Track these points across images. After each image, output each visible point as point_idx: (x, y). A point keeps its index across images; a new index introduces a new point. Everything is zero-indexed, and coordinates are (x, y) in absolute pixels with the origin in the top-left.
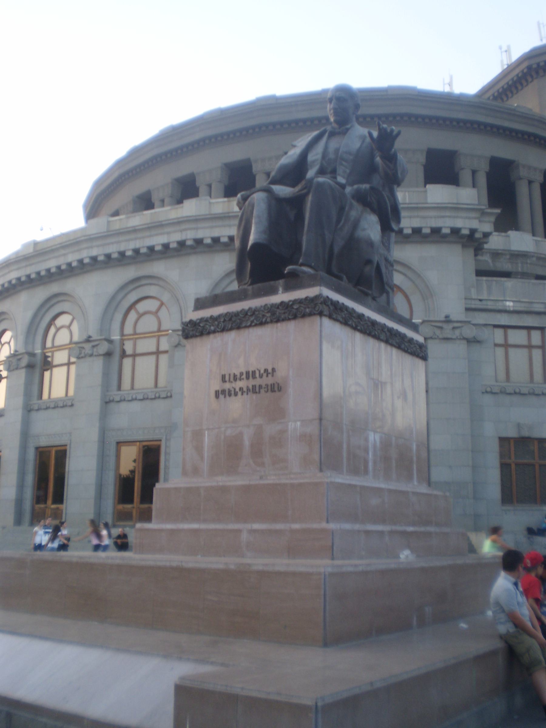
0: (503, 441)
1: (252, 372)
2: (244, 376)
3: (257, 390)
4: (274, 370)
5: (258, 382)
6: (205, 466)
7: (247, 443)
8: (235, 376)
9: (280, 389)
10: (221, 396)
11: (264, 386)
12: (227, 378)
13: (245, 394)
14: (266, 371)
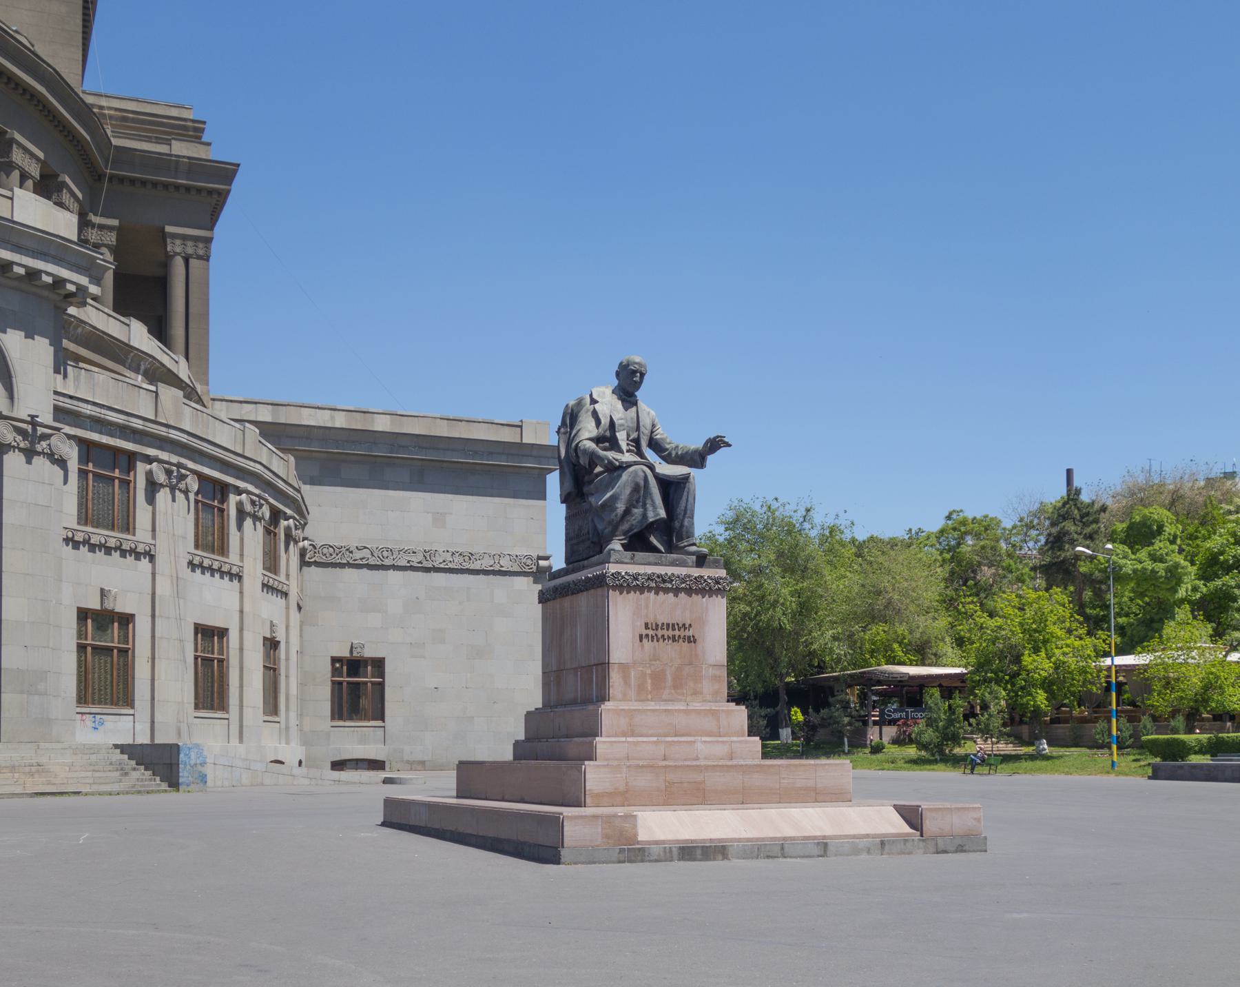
0: (83, 614)
5: (677, 633)
6: (632, 693)
7: (669, 677)
8: (657, 625)
10: (645, 640)
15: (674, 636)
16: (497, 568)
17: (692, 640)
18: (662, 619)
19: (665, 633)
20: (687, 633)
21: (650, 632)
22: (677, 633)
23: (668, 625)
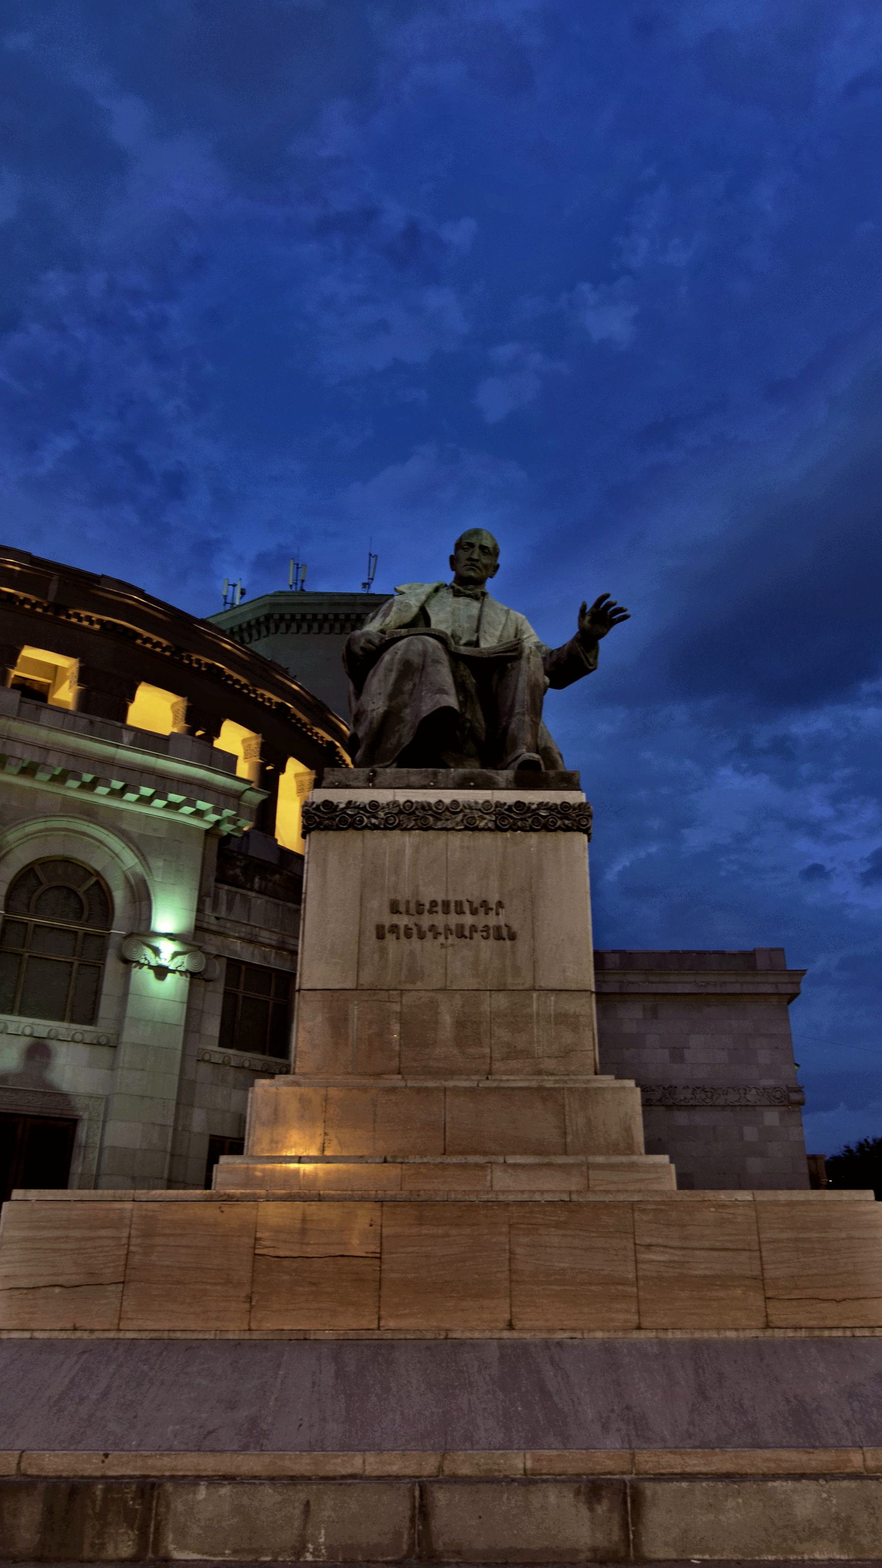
1: (456, 902)
2: (439, 908)
3: (467, 933)
4: (500, 904)
5: (468, 919)
7: (447, 1019)
8: (420, 905)
9: (513, 937)
10: (388, 936)
11: (480, 928)
12: (402, 908)
13: (442, 939)
14: (484, 903)
15: (461, 927)
16: (743, 1102)
17: (504, 935)
18: (430, 893)
19: (439, 920)
20: (492, 920)
21: (403, 921)
22: (468, 919)
23: (446, 904)
